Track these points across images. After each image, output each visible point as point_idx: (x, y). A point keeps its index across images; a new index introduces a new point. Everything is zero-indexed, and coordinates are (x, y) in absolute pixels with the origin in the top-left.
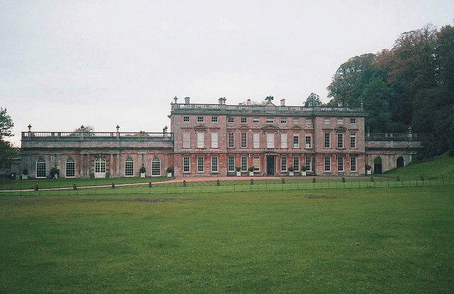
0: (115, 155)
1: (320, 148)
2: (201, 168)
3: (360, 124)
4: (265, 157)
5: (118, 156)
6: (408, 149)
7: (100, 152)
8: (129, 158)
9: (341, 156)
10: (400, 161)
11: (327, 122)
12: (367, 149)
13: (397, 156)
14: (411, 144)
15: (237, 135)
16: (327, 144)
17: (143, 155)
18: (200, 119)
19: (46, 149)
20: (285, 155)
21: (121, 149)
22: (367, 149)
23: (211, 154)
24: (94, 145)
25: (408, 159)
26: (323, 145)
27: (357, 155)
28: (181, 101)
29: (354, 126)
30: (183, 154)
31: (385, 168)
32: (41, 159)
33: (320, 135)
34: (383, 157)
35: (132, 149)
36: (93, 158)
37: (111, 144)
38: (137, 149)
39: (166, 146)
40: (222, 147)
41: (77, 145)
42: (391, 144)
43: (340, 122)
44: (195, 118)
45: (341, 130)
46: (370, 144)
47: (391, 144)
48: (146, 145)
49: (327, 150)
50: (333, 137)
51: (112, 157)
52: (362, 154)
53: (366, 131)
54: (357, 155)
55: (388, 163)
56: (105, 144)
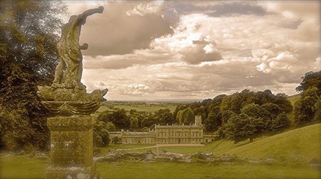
0: (142, 139)
3: (202, 130)
8: (145, 139)
9: (197, 139)
10: (212, 140)
11: (194, 130)
12: (204, 137)
15: (171, 133)
19: (127, 137)
21: (144, 137)
22: (204, 137)
24: (138, 136)
27: (202, 138)
30: (158, 138)
33: (192, 133)
35: (146, 137)
37: (142, 136)
41: (134, 136)
42: (210, 136)
43: (197, 130)
44: (161, 130)
45: (197, 132)
46: (204, 136)
47: (210, 136)
48: (149, 136)
49: (193, 137)
50: (195, 134)
53: (204, 132)
55: (209, 140)
56: (140, 136)
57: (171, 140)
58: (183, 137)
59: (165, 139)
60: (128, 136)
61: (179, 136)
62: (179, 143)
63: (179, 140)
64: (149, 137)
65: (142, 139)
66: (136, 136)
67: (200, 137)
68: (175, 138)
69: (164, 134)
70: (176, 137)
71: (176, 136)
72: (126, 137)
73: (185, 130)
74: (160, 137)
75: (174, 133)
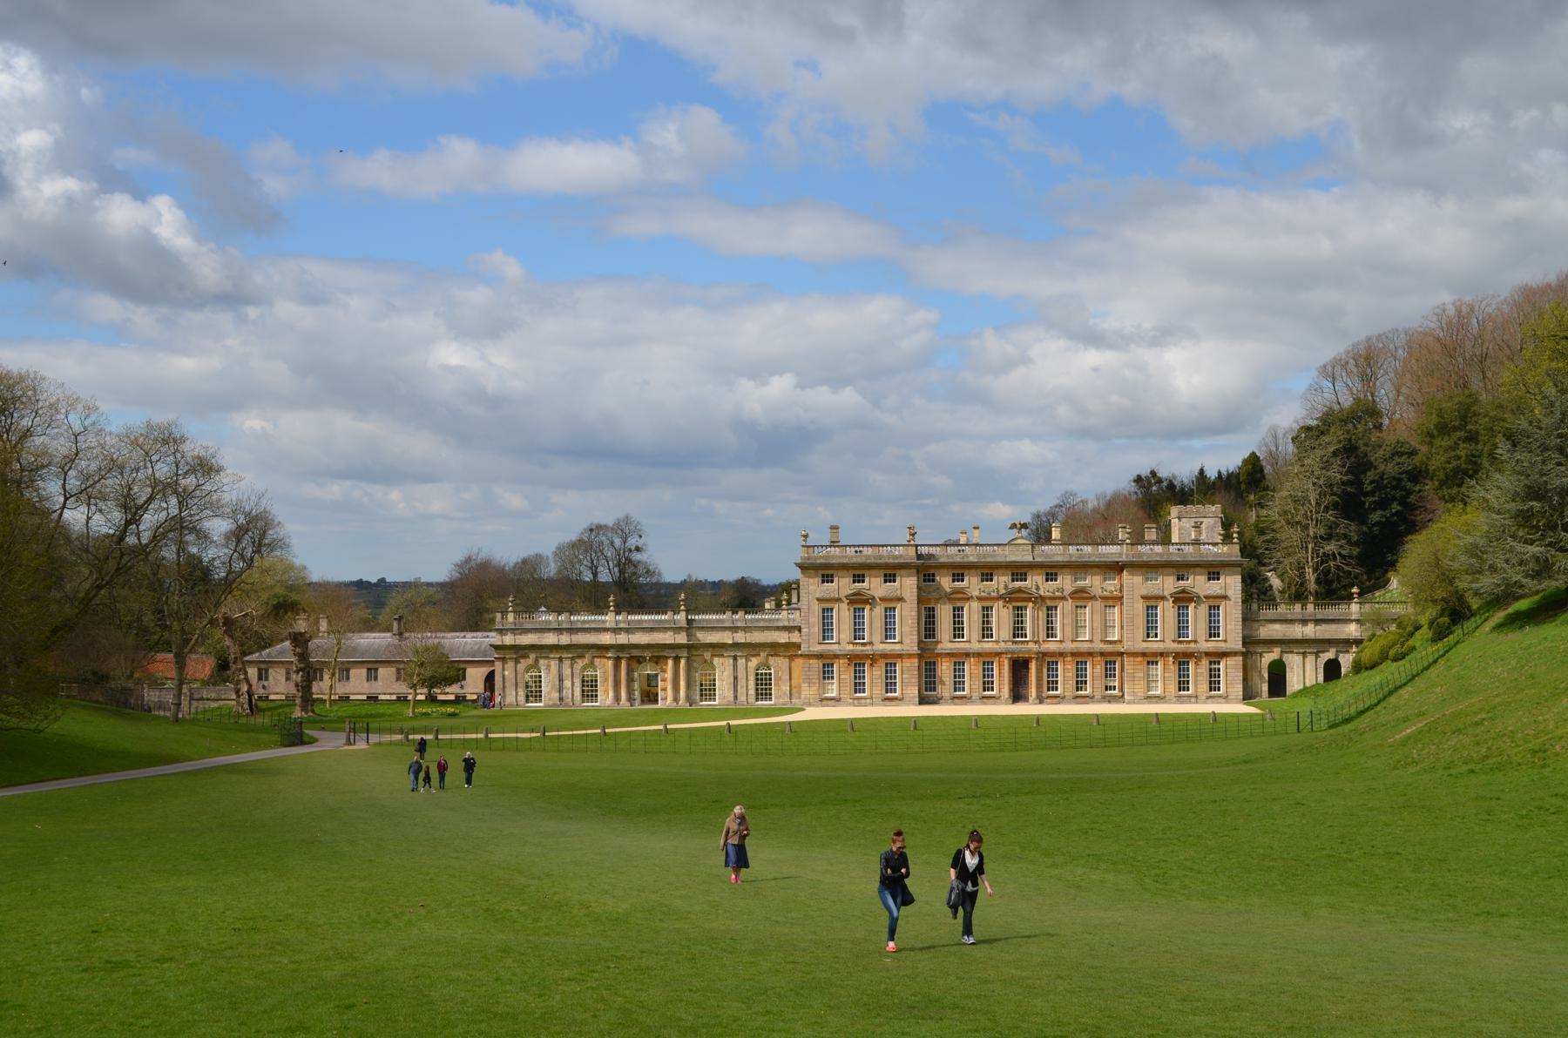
0: (677, 659)
1: (1136, 641)
2: (858, 687)
3: (1232, 584)
4: (1006, 662)
5: (683, 662)
6: (1346, 644)
7: (647, 654)
10: (1332, 670)
13: (1330, 655)
14: (1352, 630)
15: (944, 613)
16: (1150, 629)
17: (735, 658)
18: (859, 578)
20: (1049, 660)
23: (884, 656)
25: (1346, 661)
26: (1141, 633)
27: (1225, 654)
28: (821, 537)
29: (1215, 587)
30: (819, 656)
31: (1294, 682)
32: (535, 665)
34: (1288, 658)
36: (634, 664)
37: (667, 638)
38: (723, 646)
39: (782, 638)
40: (906, 640)
42: (1310, 631)
48: (740, 637)
49: (1153, 646)
51: (670, 662)
52: (1235, 654)
54: (1225, 654)
57: (945, 670)
58: (1051, 646)
59: (890, 661)
60: (550, 639)
61: (1018, 631)
62: (1017, 696)
63: (1019, 667)
64: (736, 645)
65: (677, 659)
66: (622, 639)
67: (1211, 646)
68: (979, 655)
69: (873, 617)
70: (988, 646)
71: (986, 632)
72: (533, 647)
73: (1066, 582)
74: (841, 639)
75: (972, 613)
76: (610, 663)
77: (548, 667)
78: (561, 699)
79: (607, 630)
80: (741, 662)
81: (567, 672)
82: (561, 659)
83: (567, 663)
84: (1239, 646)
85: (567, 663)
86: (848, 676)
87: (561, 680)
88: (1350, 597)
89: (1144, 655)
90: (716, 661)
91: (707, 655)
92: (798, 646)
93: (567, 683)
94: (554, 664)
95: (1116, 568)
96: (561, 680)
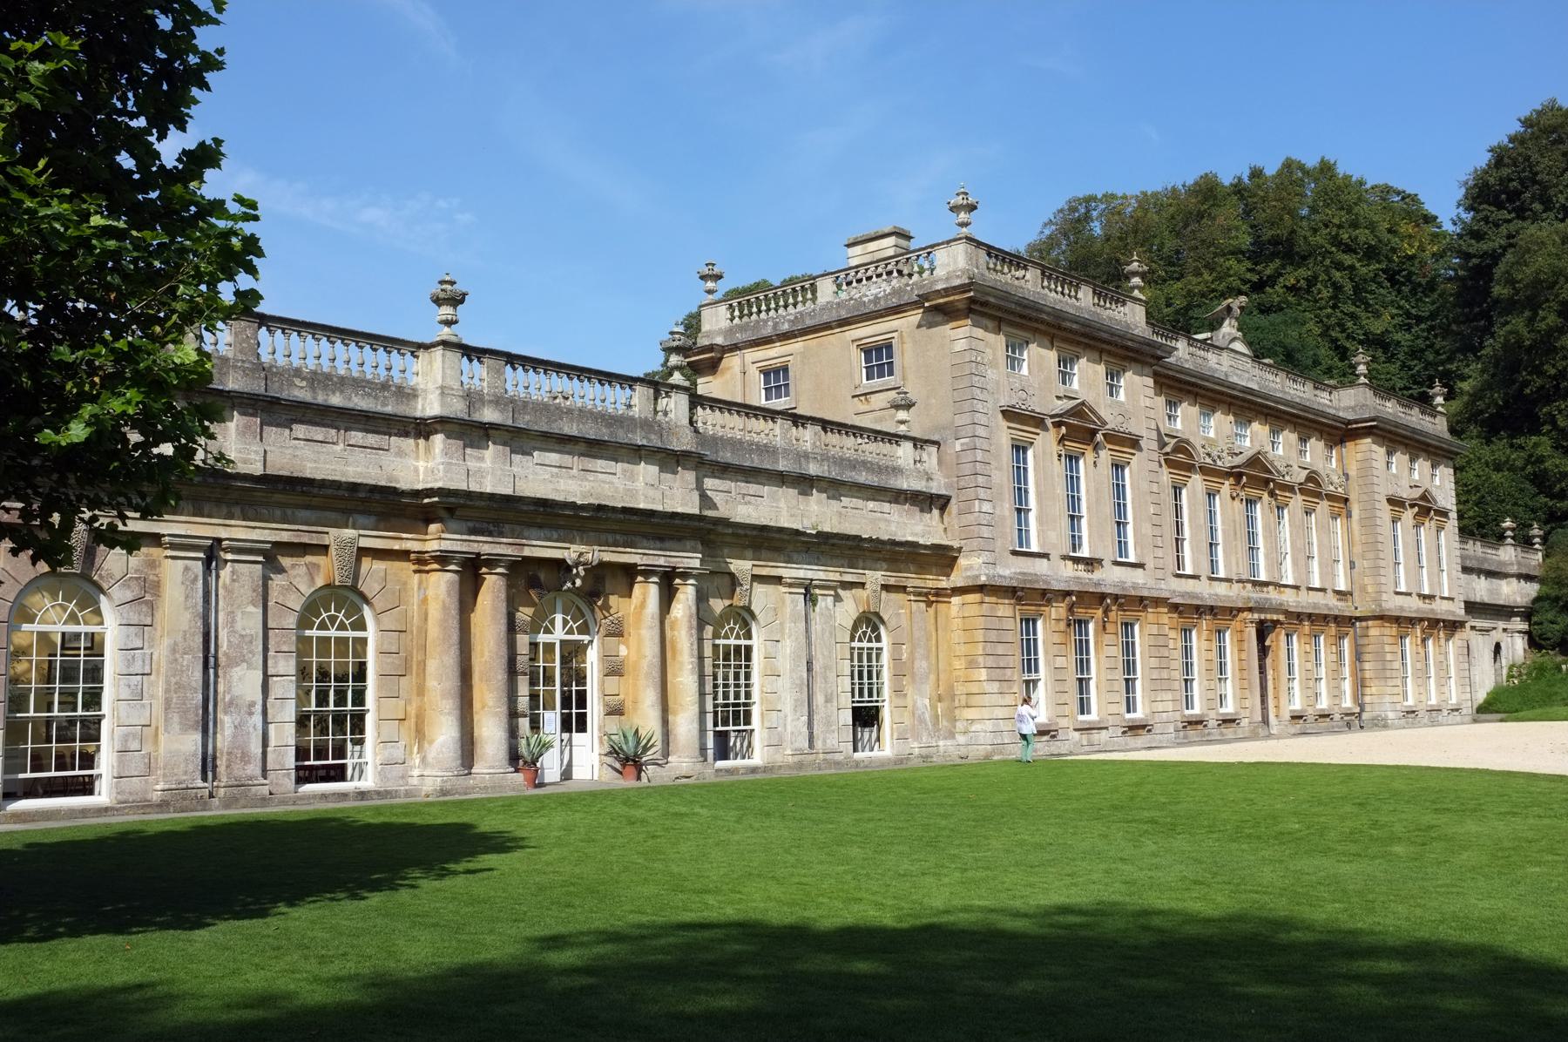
12: (1473, 608)
27: (1453, 626)
40: (1150, 565)
58: (1290, 599)
76: (441, 585)
77: (147, 593)
78: (208, 765)
79: (422, 429)
80: (825, 602)
81: (239, 620)
82: (212, 554)
83: (238, 577)
84: (1458, 611)
85: (238, 577)
86: (1069, 661)
87: (209, 662)
88: (1501, 538)
89: (1396, 620)
90: (761, 598)
91: (741, 566)
92: (943, 558)
93: (242, 682)
94: (176, 576)
95: (1339, 433)
96: (209, 662)
